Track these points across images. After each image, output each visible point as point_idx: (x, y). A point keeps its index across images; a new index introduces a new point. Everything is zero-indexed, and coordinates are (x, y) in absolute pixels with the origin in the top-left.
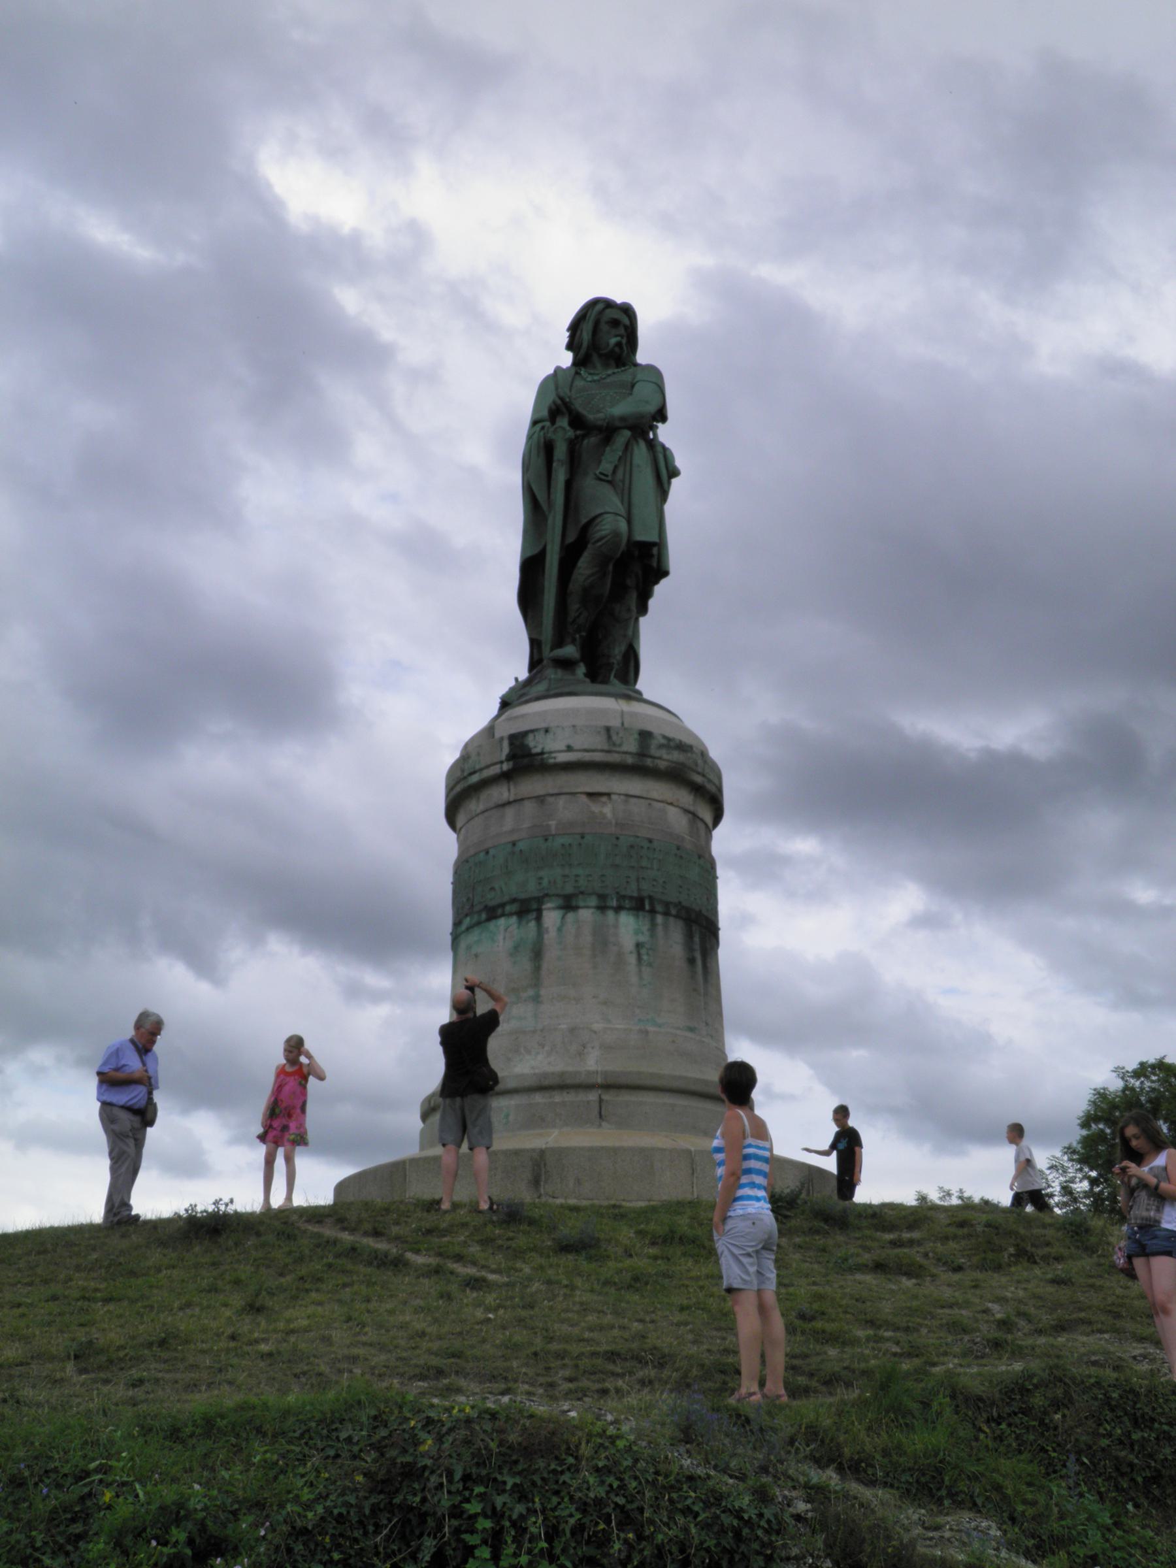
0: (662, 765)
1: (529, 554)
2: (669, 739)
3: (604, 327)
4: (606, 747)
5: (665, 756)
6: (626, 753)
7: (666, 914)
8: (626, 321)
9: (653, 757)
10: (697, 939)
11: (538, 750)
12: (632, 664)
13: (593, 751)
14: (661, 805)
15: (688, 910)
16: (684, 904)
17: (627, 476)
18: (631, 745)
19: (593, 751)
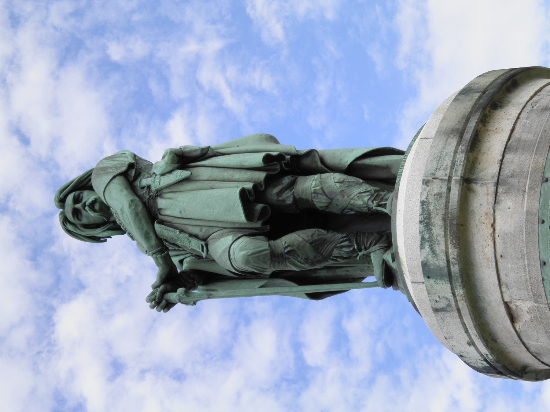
0: (453, 252)
1: (305, 296)
2: (423, 239)
3: (85, 221)
4: (456, 314)
5: (443, 247)
6: (454, 294)
8: (70, 198)
9: (448, 261)
11: (485, 364)
12: (367, 161)
13: (464, 325)
14: (498, 240)
17: (194, 223)
18: (443, 288)
19: (464, 325)
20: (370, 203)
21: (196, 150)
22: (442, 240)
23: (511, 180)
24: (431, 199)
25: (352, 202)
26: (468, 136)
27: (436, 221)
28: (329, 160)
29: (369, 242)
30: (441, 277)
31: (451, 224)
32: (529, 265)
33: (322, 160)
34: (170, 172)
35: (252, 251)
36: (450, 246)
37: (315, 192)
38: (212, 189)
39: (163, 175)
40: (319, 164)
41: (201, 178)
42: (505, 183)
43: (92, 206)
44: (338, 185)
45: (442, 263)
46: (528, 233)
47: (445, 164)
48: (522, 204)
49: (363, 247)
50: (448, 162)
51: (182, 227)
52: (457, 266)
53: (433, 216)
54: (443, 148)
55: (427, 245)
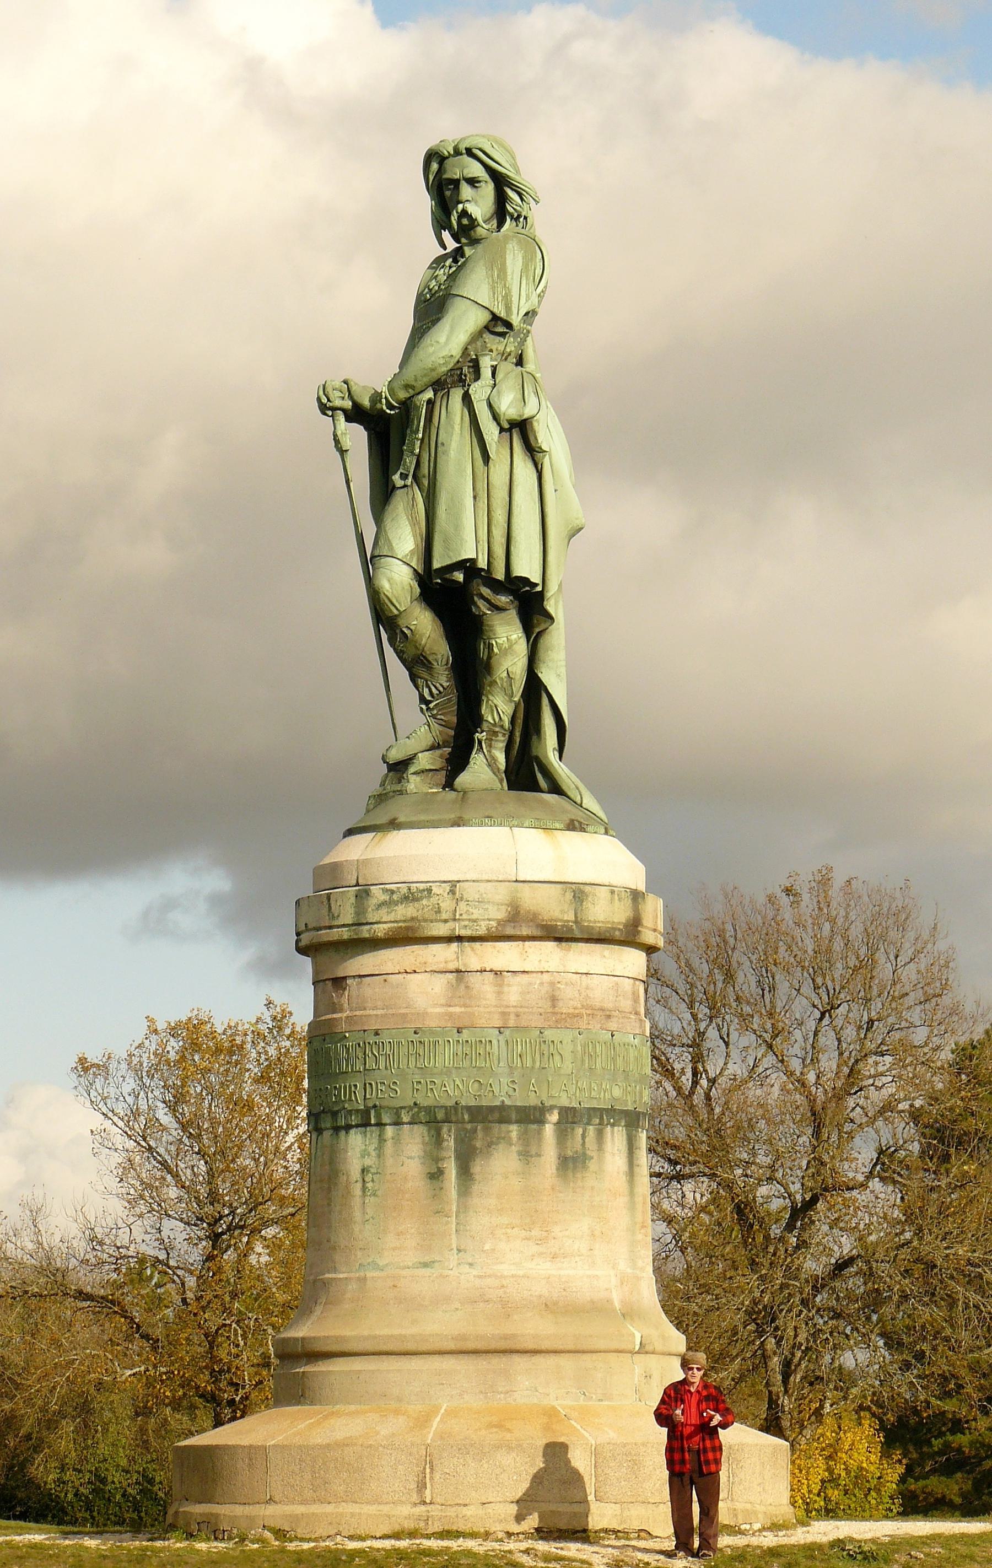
0: (381, 930)
2: (392, 892)
6: (344, 926)
7: (398, 1123)
8: (476, 170)
10: (450, 1143)
15: (429, 1110)
16: (424, 1102)
20: (485, 726)
21: (536, 439)
22: (391, 917)
23: (462, 987)
24: (434, 900)
25: (483, 698)
26: (509, 931)
27: (410, 909)
28: (543, 642)
29: (442, 717)
30: (357, 914)
31: (407, 928)
32: (377, 1015)
33: (540, 634)
34: (495, 417)
35: (390, 595)
36: (385, 926)
37: (490, 647)
38: (475, 497)
39: (490, 406)
40: (537, 630)
41: (492, 470)
42: (459, 980)
43: (464, 213)
44: (505, 674)
45: (371, 917)
46: (404, 1016)
47: (474, 911)
48: (435, 1005)
49: (435, 712)
50: (476, 914)
51: (426, 440)
52: (368, 936)
53: (416, 904)
54: (493, 903)
55: (386, 897)
